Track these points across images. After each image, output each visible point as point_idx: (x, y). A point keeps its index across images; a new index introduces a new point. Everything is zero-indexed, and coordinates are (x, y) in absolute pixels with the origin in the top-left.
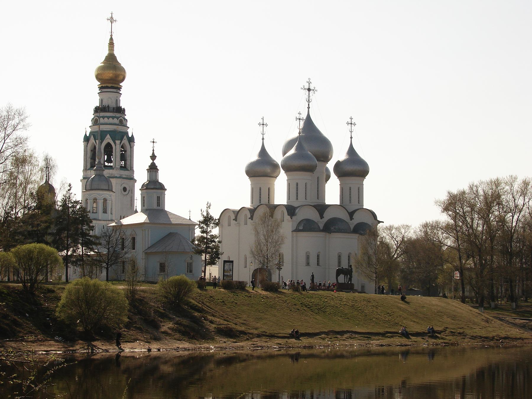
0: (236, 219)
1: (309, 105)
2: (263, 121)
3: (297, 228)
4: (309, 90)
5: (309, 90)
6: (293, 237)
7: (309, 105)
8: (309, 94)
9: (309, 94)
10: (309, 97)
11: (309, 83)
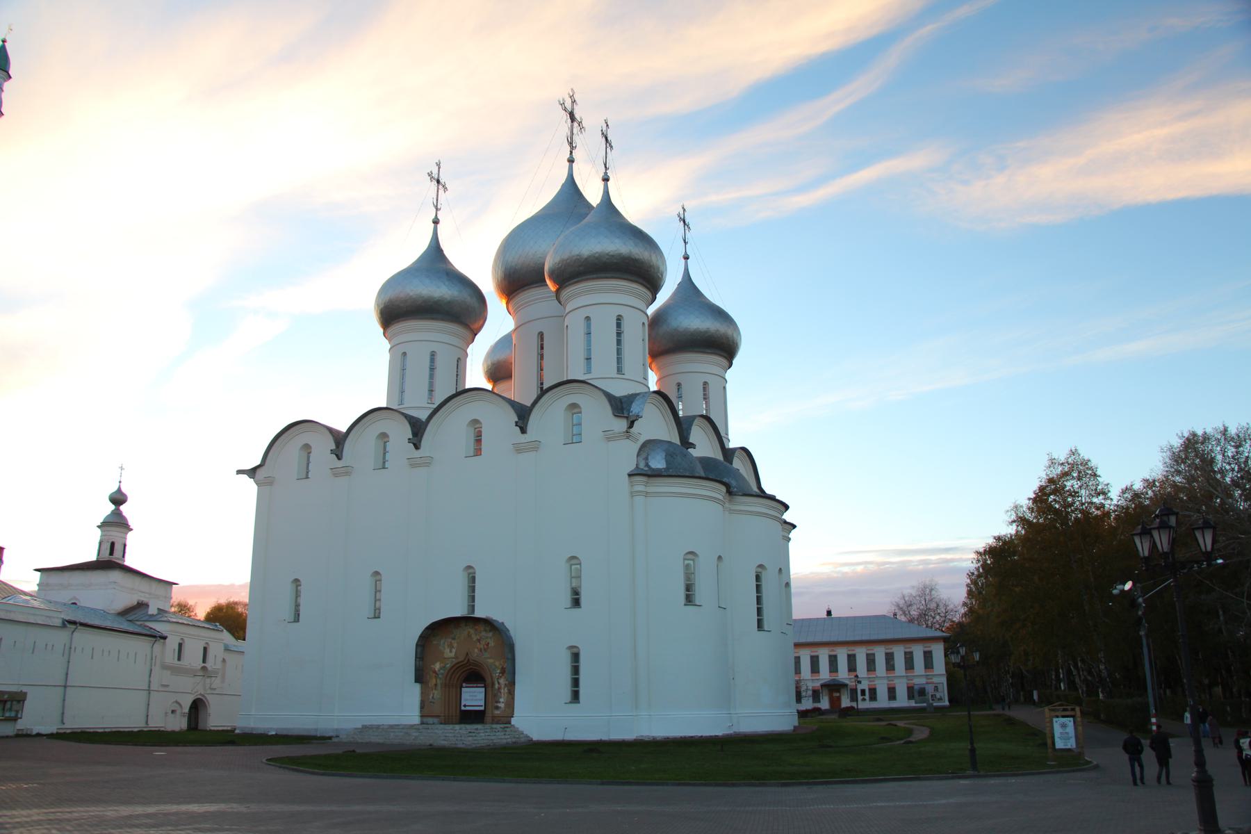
0: (338, 453)
1: (571, 152)
2: (439, 171)
3: (642, 465)
4: (572, 116)
5: (572, 116)
6: (633, 494)
7: (571, 152)
8: (572, 126)
9: (572, 126)
10: (572, 133)
11: (574, 102)
